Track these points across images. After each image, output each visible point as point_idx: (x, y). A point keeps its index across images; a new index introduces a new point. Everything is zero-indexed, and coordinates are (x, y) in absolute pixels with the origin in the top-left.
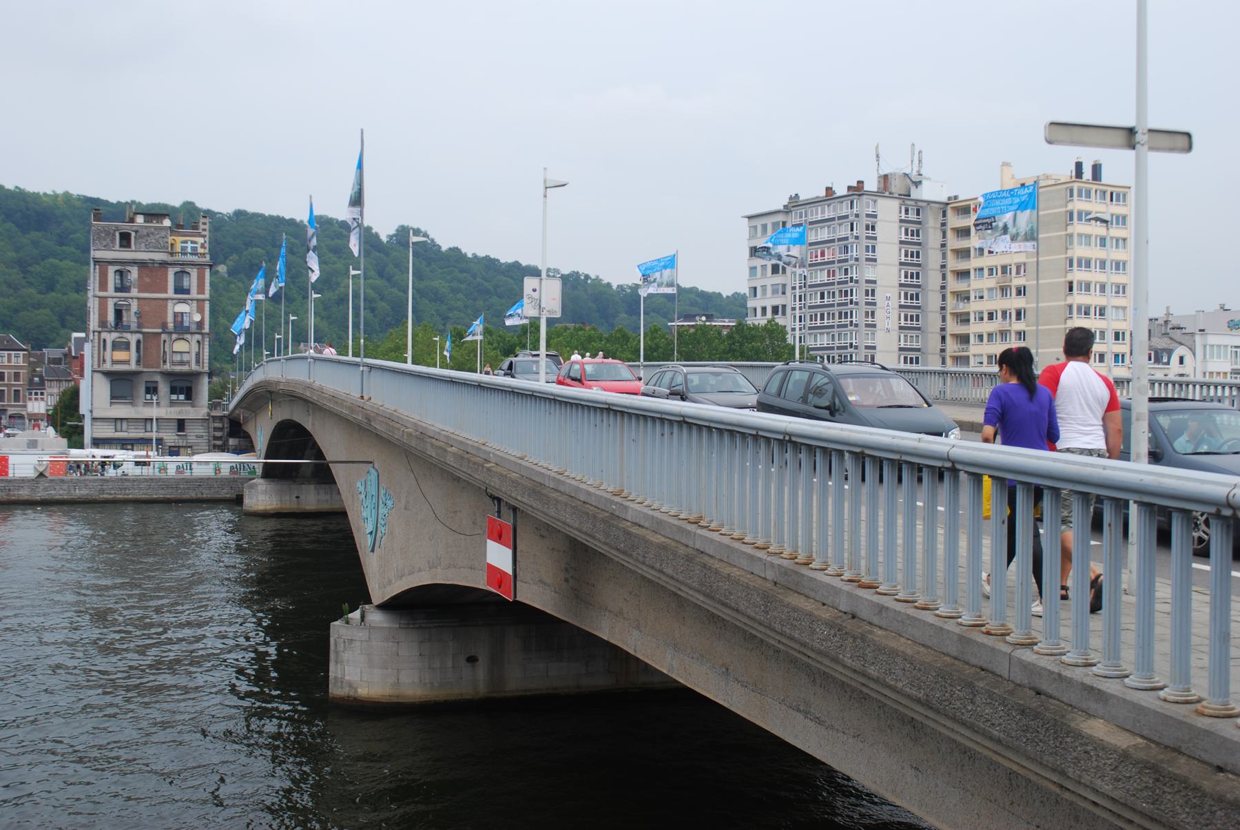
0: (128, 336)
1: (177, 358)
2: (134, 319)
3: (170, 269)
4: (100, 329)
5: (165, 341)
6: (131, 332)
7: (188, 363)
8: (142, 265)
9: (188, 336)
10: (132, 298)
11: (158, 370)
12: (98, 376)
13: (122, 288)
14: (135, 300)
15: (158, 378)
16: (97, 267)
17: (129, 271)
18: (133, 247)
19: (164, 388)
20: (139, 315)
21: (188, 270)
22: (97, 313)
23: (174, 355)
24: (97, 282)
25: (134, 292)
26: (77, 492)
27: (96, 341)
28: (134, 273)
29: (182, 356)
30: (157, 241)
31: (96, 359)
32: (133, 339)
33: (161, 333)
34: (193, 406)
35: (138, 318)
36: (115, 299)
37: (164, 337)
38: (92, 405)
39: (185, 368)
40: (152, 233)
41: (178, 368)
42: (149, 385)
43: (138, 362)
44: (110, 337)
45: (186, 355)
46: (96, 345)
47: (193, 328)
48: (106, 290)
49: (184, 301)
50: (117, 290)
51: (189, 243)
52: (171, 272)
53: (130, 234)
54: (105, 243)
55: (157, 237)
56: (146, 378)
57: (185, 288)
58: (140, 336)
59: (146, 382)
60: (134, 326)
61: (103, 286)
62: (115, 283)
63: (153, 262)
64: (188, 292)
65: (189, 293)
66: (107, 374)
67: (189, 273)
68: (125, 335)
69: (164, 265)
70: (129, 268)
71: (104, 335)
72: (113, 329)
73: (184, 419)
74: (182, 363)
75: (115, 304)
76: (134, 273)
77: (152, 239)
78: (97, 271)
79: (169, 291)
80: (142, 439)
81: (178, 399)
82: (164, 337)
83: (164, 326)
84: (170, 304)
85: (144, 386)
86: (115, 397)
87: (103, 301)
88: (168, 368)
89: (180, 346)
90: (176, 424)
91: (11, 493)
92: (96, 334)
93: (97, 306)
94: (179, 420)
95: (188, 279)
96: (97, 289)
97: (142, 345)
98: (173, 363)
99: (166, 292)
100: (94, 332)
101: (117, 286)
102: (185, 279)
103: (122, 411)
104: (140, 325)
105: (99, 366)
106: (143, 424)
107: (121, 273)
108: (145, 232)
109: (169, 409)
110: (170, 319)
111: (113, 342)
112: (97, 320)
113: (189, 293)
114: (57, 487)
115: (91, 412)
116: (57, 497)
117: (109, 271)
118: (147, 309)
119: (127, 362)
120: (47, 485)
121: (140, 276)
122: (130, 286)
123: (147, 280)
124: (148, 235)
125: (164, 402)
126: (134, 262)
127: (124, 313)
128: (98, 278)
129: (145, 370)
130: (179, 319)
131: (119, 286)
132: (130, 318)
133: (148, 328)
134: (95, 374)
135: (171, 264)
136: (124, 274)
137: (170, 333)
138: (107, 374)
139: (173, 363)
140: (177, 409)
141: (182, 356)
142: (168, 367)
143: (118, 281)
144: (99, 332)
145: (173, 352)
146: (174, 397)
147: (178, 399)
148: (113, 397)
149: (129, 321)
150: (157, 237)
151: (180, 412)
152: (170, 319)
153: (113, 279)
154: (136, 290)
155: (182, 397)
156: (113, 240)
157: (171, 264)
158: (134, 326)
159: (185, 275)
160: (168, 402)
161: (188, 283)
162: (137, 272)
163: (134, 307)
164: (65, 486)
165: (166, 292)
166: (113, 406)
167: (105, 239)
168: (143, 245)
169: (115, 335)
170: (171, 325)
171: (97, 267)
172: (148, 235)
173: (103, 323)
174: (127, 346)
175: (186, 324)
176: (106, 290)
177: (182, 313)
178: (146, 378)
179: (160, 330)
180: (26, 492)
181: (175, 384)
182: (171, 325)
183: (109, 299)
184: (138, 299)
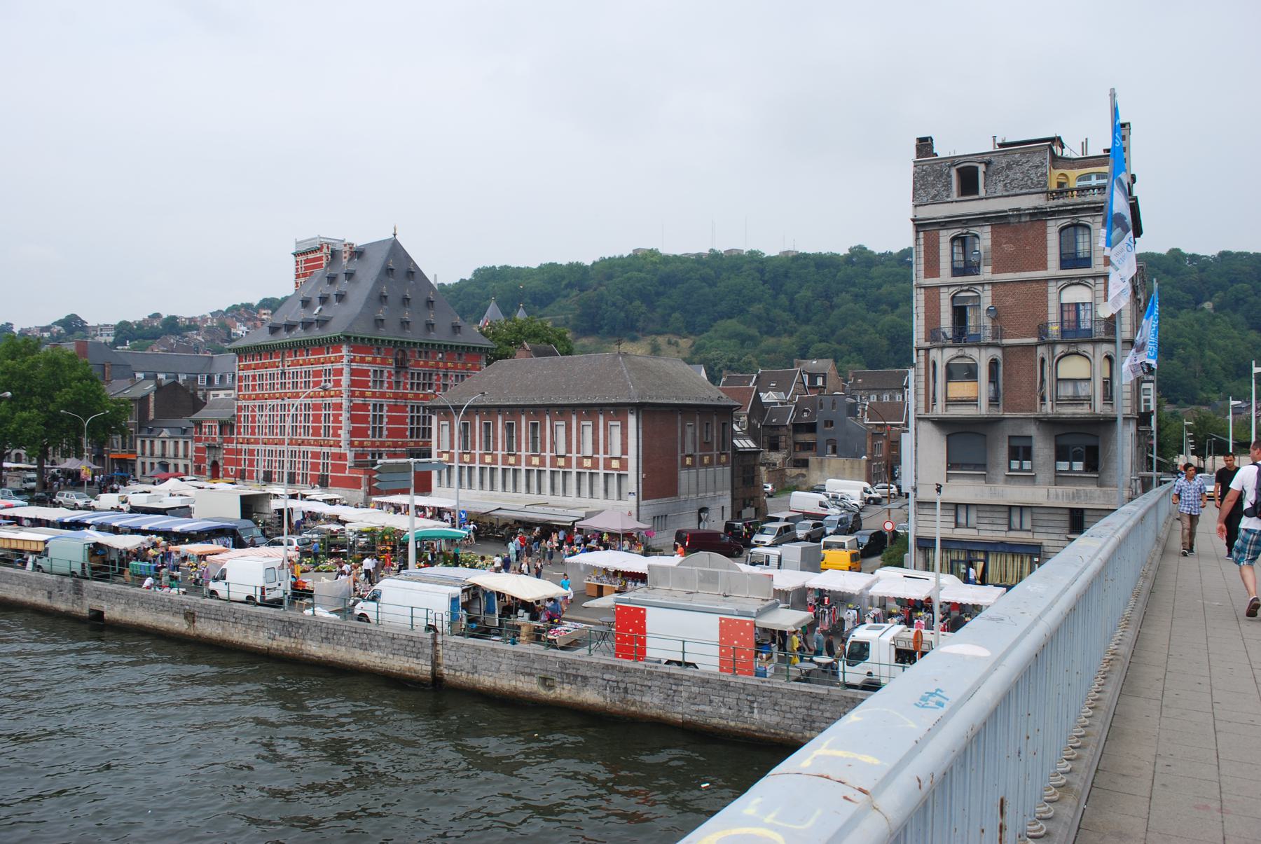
0: (973, 353)
1: (1067, 391)
2: (986, 321)
3: (1050, 223)
4: (928, 344)
5: (1043, 360)
6: (979, 346)
7: (1089, 400)
8: (997, 220)
9: (1088, 348)
10: (982, 284)
11: (1032, 415)
12: (926, 428)
13: (966, 268)
14: (987, 287)
15: (1032, 430)
16: (921, 235)
17: (977, 236)
18: (982, 192)
19: (1043, 449)
20: (995, 313)
21: (1086, 220)
22: (922, 316)
23: (1061, 386)
24: (922, 261)
25: (986, 273)
26: (756, 715)
27: (922, 365)
28: (985, 238)
29: (1075, 387)
30: (1026, 174)
31: (922, 398)
32: (982, 358)
33: (1037, 345)
34: (1101, 485)
35: (994, 320)
36: (952, 289)
37: (1041, 351)
38: (916, 478)
39: (1082, 411)
40: (1017, 163)
41: (1068, 411)
42: (1016, 443)
43: (994, 401)
44: (942, 357)
45: (1083, 384)
46: (922, 372)
47: (1100, 332)
48: (938, 276)
49: (1080, 281)
50: (956, 272)
51: (1094, 177)
52: (1053, 230)
53: (977, 168)
54: (933, 192)
55: (1026, 167)
56: (1009, 430)
57: (1081, 255)
58: (998, 353)
59: (1010, 437)
60: (987, 335)
61: (932, 268)
62: (953, 261)
63: (1019, 213)
64: (1086, 262)
65: (1089, 266)
66: (941, 423)
67: (1088, 227)
68: (968, 351)
69: (1039, 215)
70: (975, 230)
71: (934, 354)
72: (950, 342)
73: (1082, 510)
74: (1076, 400)
75: (953, 298)
76: (985, 238)
77: (1016, 173)
78: (922, 241)
79: (1050, 264)
80: (1002, 543)
81: (1071, 470)
82: (1041, 351)
83: (1042, 330)
84: (1052, 289)
85: (1006, 445)
86: (953, 464)
87: (932, 292)
88: (1049, 411)
89: (1072, 368)
90: (1067, 518)
91: (629, 697)
92: (922, 353)
93: (922, 303)
94: (1072, 510)
95: (1087, 239)
96: (922, 273)
97: (1001, 368)
98: (1058, 401)
99: (1045, 268)
100: (918, 350)
101: (956, 265)
102: (1080, 239)
103: (966, 490)
104: (997, 333)
105: (927, 410)
106: (1006, 515)
107: (961, 241)
108: (1004, 161)
109: (1053, 489)
110: (1053, 316)
111: (948, 365)
112: (922, 329)
113: (1089, 266)
114: (716, 699)
115: (915, 490)
116: (715, 721)
117: (941, 239)
118: (1009, 301)
119: (973, 402)
120: (695, 689)
121: (995, 243)
122: (979, 264)
123: (1009, 248)
124: (1009, 167)
125: (1044, 474)
126: (983, 219)
127: (970, 313)
128: (922, 254)
129: (1007, 415)
130: (1072, 316)
131: (962, 265)
132: (980, 321)
133: (1013, 336)
134: (922, 425)
135: (1052, 213)
136: (969, 241)
137: (1053, 344)
138: (941, 423)
139: (1058, 401)
140: (1069, 489)
141: (1075, 387)
142: (1048, 409)
143: (959, 257)
144: (927, 350)
145: (1058, 380)
146: (1063, 466)
147: (1071, 470)
148: (951, 465)
149: (978, 327)
150: (1026, 167)
151: (1075, 496)
152: (1053, 316)
153: (949, 252)
154: (989, 269)
155: (1078, 466)
156: (948, 186)
157: (1052, 213)
158: (987, 335)
159: (1080, 231)
160: (1051, 475)
161: (1087, 247)
162: (989, 236)
163: (987, 299)
164: (731, 700)
165: (1045, 268)
166: (953, 481)
167: (934, 186)
168: (1000, 186)
169: (950, 353)
170: (1054, 329)
171: (921, 235)
172: (1009, 167)
173: (933, 333)
174: (970, 373)
175: (1086, 325)
176: (938, 276)
177: (1077, 304)
178: (1009, 430)
179: (1034, 340)
180: (656, 701)
181: (1065, 441)
182: (1054, 329)
183: (942, 290)
184: (993, 284)
